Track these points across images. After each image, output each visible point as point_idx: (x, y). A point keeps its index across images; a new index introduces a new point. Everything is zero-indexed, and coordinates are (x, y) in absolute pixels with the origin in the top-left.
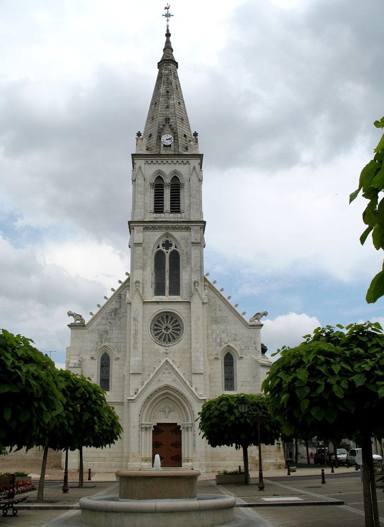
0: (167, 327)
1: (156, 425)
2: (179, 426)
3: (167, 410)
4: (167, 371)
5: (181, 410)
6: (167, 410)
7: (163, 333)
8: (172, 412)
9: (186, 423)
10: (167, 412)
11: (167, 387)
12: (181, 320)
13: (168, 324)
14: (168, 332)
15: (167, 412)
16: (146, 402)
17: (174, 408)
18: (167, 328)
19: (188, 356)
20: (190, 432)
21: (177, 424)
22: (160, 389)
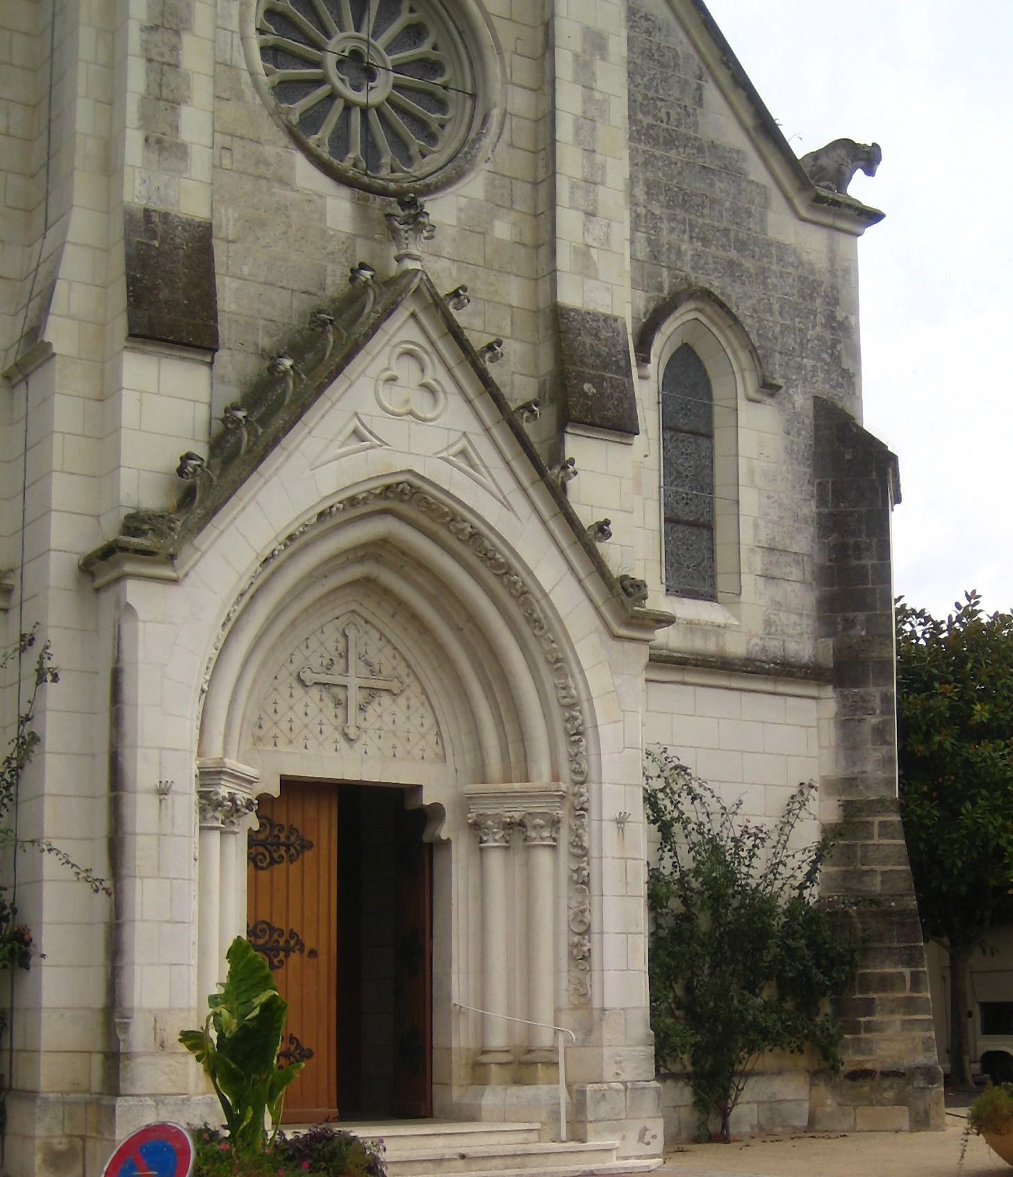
0: (356, 55)
1: (275, 791)
2: (436, 812)
3: (353, 682)
4: (407, 372)
5: (464, 696)
6: (353, 682)
7: (332, 96)
8: (386, 699)
9: (517, 786)
10: (355, 697)
11: (403, 496)
12: (468, 31)
13: (380, 43)
14: (359, 97)
15: (355, 697)
16: (251, 597)
17: (402, 670)
18: (359, 67)
19: (515, 302)
20: (543, 859)
21: (417, 789)
22: (354, 506)
